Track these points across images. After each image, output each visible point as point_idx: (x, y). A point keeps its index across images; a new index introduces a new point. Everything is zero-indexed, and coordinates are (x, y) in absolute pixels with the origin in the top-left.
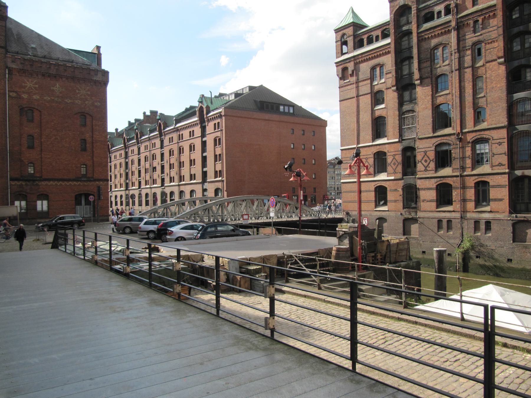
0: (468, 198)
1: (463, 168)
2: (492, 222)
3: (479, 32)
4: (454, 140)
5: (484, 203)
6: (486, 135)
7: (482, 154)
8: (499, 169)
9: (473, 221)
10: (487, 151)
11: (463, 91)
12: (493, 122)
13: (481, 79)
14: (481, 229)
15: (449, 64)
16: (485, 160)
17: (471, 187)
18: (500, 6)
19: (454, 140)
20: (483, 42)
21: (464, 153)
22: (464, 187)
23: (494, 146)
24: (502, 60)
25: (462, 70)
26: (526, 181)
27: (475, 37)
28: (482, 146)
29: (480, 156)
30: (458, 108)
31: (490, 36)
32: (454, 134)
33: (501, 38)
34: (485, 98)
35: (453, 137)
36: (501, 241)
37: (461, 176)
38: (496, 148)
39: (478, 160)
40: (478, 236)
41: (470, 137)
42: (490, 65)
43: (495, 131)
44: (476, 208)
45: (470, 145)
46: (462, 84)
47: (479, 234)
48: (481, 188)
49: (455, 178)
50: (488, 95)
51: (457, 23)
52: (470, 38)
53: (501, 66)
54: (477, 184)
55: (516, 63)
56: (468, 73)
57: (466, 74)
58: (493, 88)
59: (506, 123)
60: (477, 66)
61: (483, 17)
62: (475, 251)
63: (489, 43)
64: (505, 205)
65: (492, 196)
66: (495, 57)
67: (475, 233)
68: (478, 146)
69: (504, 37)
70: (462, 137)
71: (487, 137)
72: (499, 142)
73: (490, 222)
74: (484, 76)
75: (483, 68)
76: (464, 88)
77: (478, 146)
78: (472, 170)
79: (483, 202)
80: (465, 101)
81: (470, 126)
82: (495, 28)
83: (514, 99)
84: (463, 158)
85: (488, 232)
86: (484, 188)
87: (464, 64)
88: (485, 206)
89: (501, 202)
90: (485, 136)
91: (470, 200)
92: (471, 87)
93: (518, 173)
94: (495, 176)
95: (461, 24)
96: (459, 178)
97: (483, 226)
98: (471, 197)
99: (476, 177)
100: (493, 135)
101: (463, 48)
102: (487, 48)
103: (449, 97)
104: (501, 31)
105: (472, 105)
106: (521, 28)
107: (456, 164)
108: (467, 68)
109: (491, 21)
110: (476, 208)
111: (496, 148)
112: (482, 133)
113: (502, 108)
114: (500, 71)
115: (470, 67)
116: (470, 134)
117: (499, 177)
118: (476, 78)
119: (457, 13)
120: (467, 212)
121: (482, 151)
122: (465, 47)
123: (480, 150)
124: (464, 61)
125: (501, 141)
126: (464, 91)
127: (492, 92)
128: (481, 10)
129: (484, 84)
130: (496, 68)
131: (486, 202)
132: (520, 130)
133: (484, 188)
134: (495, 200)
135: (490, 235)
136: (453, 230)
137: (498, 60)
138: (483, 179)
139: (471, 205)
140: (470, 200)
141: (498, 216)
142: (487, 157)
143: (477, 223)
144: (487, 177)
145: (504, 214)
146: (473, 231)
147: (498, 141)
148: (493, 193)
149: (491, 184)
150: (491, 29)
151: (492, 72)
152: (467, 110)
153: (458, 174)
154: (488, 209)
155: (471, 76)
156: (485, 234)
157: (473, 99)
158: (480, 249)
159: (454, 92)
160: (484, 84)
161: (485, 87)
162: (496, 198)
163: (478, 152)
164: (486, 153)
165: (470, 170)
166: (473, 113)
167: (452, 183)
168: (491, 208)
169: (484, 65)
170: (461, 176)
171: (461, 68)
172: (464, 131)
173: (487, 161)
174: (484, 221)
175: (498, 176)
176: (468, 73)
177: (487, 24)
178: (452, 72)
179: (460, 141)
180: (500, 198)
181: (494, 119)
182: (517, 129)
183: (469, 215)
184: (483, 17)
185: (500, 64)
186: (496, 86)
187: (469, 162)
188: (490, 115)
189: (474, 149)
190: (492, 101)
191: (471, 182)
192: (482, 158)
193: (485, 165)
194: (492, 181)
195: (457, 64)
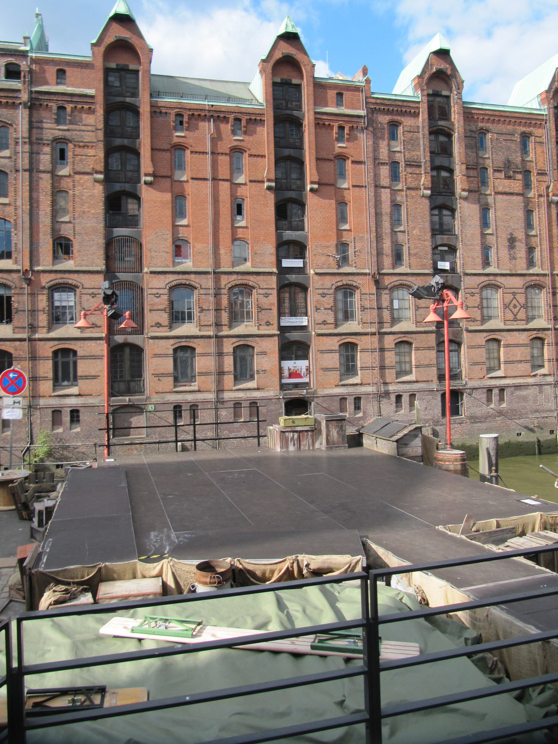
0: (42, 376)
1: (33, 328)
2: (82, 410)
3: (65, 124)
4: (17, 282)
5: (66, 383)
6: (72, 279)
7: (64, 307)
8: (92, 332)
9: (50, 411)
10: (72, 304)
11: (35, 205)
12: (84, 263)
13: (64, 194)
14: (63, 421)
15: (10, 158)
16: (68, 317)
17: (47, 358)
18: (100, 99)
19: (17, 282)
20: (71, 142)
21: (33, 303)
22: (34, 358)
23: (85, 298)
24: (101, 177)
25: (34, 174)
26: (127, 350)
27: (59, 130)
28: (64, 295)
29: (60, 310)
30: (27, 232)
31: (82, 136)
32: (18, 271)
33: (101, 145)
34: (71, 225)
35: (15, 276)
36: (95, 437)
37: (30, 340)
38: (88, 300)
39: (57, 317)
40: (58, 433)
41: (45, 280)
42: (81, 179)
43: (87, 276)
44: (54, 390)
45: (46, 292)
46: (35, 195)
47: (60, 430)
48: (60, 359)
49: (18, 343)
50: (77, 221)
51: (31, 99)
52: (51, 129)
53: (96, 184)
54: (56, 353)
55: (118, 187)
56: (45, 181)
57: (41, 182)
58: (84, 212)
59: (104, 267)
60: (61, 173)
61: (73, 106)
62: (54, 457)
63: (80, 146)
64: (102, 384)
65: (80, 373)
66: (88, 170)
67: (53, 430)
68: (57, 295)
69: (104, 145)
70: (33, 278)
71: (74, 283)
72: (93, 293)
73: (78, 411)
74: (71, 192)
75: (69, 180)
76: (38, 202)
77: (57, 295)
78: (49, 331)
79: (63, 381)
80: (38, 222)
81: (45, 262)
82: (93, 128)
83: (115, 235)
84: (33, 312)
85: (74, 426)
86: (65, 360)
87: (38, 164)
88: (68, 387)
89: (94, 380)
90: (70, 282)
91: (45, 379)
92: (49, 202)
93: (119, 339)
94: (87, 342)
95: (37, 103)
96: (26, 344)
97: (66, 418)
98: (47, 373)
99: (56, 342)
100: (83, 281)
101: (37, 139)
102: (76, 153)
103: (10, 210)
104: (101, 135)
105: (49, 230)
106: (126, 142)
107: (21, 319)
108: (44, 172)
109: (84, 116)
110: (54, 390)
111: (88, 300)
112: (67, 276)
113: (98, 244)
114: (96, 191)
115: (48, 172)
116: (46, 275)
117: (93, 343)
118: (57, 192)
119: (31, 83)
120: (40, 397)
121: (64, 304)
122: (42, 139)
123: (61, 301)
124: (38, 161)
125: (95, 291)
126: (37, 207)
127: (83, 218)
128: (72, 95)
129: (71, 204)
130: (89, 184)
131: (68, 380)
132: (121, 280)
133: (65, 360)
134: (86, 377)
135: (78, 430)
136: (11, 428)
137: (95, 175)
138: (66, 346)
139: (46, 387)
140: (45, 379)
141: (90, 401)
142: (71, 313)
143: (57, 413)
144: (73, 342)
145: (100, 398)
146: (50, 426)
147: (91, 291)
148: (83, 368)
149: (80, 353)
150: (84, 128)
151: (84, 189)
152: (41, 236)
153: (25, 336)
154: (74, 390)
155: (49, 187)
156: (71, 429)
157: (52, 222)
158: (62, 455)
159: (19, 203)
160: (71, 204)
161: (71, 209)
162: (87, 374)
163: (57, 304)
164: (71, 307)
165: (45, 330)
166: (51, 242)
167: (11, 351)
168: (80, 391)
169: (69, 176)
170: (30, 340)
171: (32, 169)
172: (36, 269)
173: (72, 319)
174: (69, 409)
175: (91, 342)
176: (45, 181)
177: (77, 119)
178: (17, 171)
179: (28, 285)
180: (93, 374)
181: (85, 258)
182: (117, 278)
183: (42, 402)
184: (73, 106)
185: (96, 181)
186: (89, 212)
187: (43, 319)
188: (79, 251)
189: (51, 299)
190: (82, 232)
191: (47, 349)
192: (64, 313)
193: (68, 325)
194: (81, 348)
195: (27, 161)
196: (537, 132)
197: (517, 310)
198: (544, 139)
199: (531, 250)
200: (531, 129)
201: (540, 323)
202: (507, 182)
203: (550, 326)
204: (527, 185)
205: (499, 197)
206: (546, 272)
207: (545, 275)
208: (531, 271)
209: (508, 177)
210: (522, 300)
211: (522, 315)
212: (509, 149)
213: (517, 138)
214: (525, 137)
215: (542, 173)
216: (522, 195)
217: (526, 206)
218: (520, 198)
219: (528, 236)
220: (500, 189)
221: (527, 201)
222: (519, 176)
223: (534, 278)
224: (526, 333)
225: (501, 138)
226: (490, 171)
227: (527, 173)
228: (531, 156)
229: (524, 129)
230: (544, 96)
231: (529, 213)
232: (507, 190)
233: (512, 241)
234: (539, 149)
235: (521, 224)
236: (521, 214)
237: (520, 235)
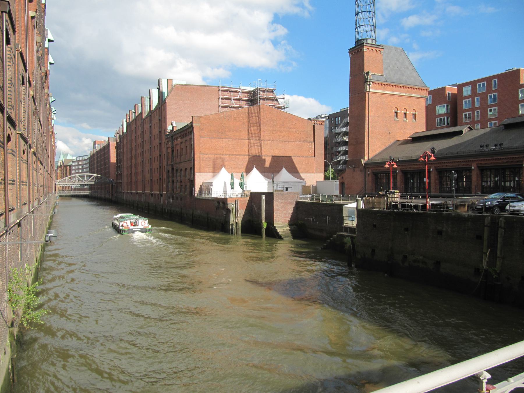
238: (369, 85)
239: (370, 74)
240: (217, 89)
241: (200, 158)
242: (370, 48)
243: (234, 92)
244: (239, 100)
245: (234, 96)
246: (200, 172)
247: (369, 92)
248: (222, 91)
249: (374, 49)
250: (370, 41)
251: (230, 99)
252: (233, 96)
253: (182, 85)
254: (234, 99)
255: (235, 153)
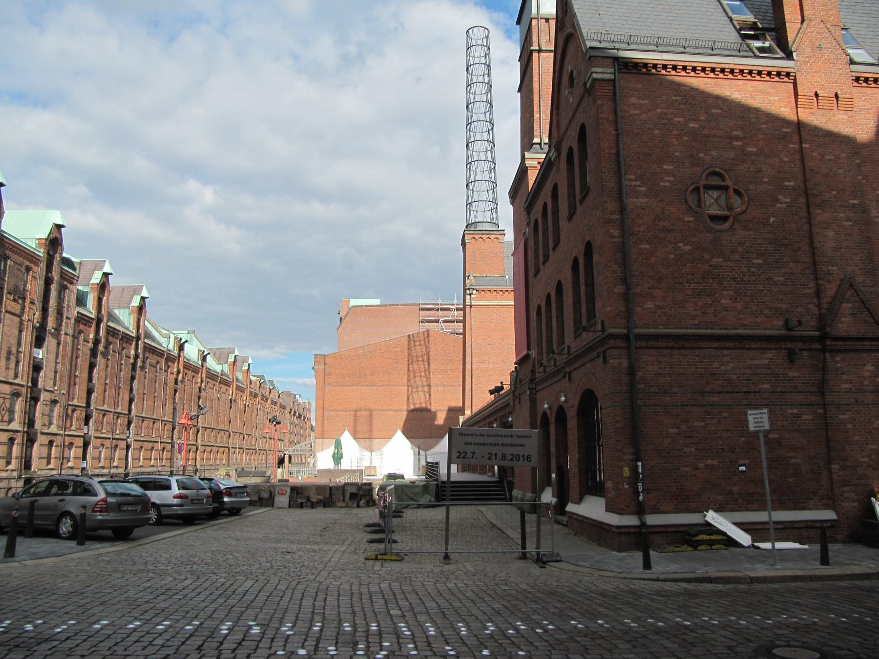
196: (35, 268)
197: (3, 413)
198: (37, 275)
199: (18, 362)
200: (31, 265)
201: (15, 425)
202: (13, 303)
203: (21, 429)
204: (23, 308)
205: (7, 315)
206: (25, 384)
207: (23, 386)
208: (16, 381)
209: (14, 300)
210: (8, 405)
211: (6, 418)
212: (18, 276)
213: (23, 269)
214: (28, 269)
215: (32, 303)
216: (20, 316)
217: (20, 326)
218: (18, 319)
219: (18, 352)
220: (8, 308)
221: (21, 323)
222: (20, 301)
223: (17, 387)
224: (6, 434)
225: (17, 266)
226: (5, 292)
227: (24, 299)
228: (28, 287)
229: (28, 263)
230: (43, 242)
231: (21, 331)
232: (12, 310)
233: (9, 353)
234: (33, 283)
235: (14, 341)
236: (16, 332)
237: (14, 351)
238: (470, 294)
239: (471, 277)
240: (417, 308)
241: (323, 416)
242: (477, 237)
243: (442, 309)
244: (454, 322)
245: (442, 317)
246: (323, 438)
247: (471, 306)
248: (422, 310)
249: (485, 237)
250: (480, 227)
251: (437, 322)
252: (443, 316)
253: (361, 306)
254: (445, 322)
255: (381, 408)
